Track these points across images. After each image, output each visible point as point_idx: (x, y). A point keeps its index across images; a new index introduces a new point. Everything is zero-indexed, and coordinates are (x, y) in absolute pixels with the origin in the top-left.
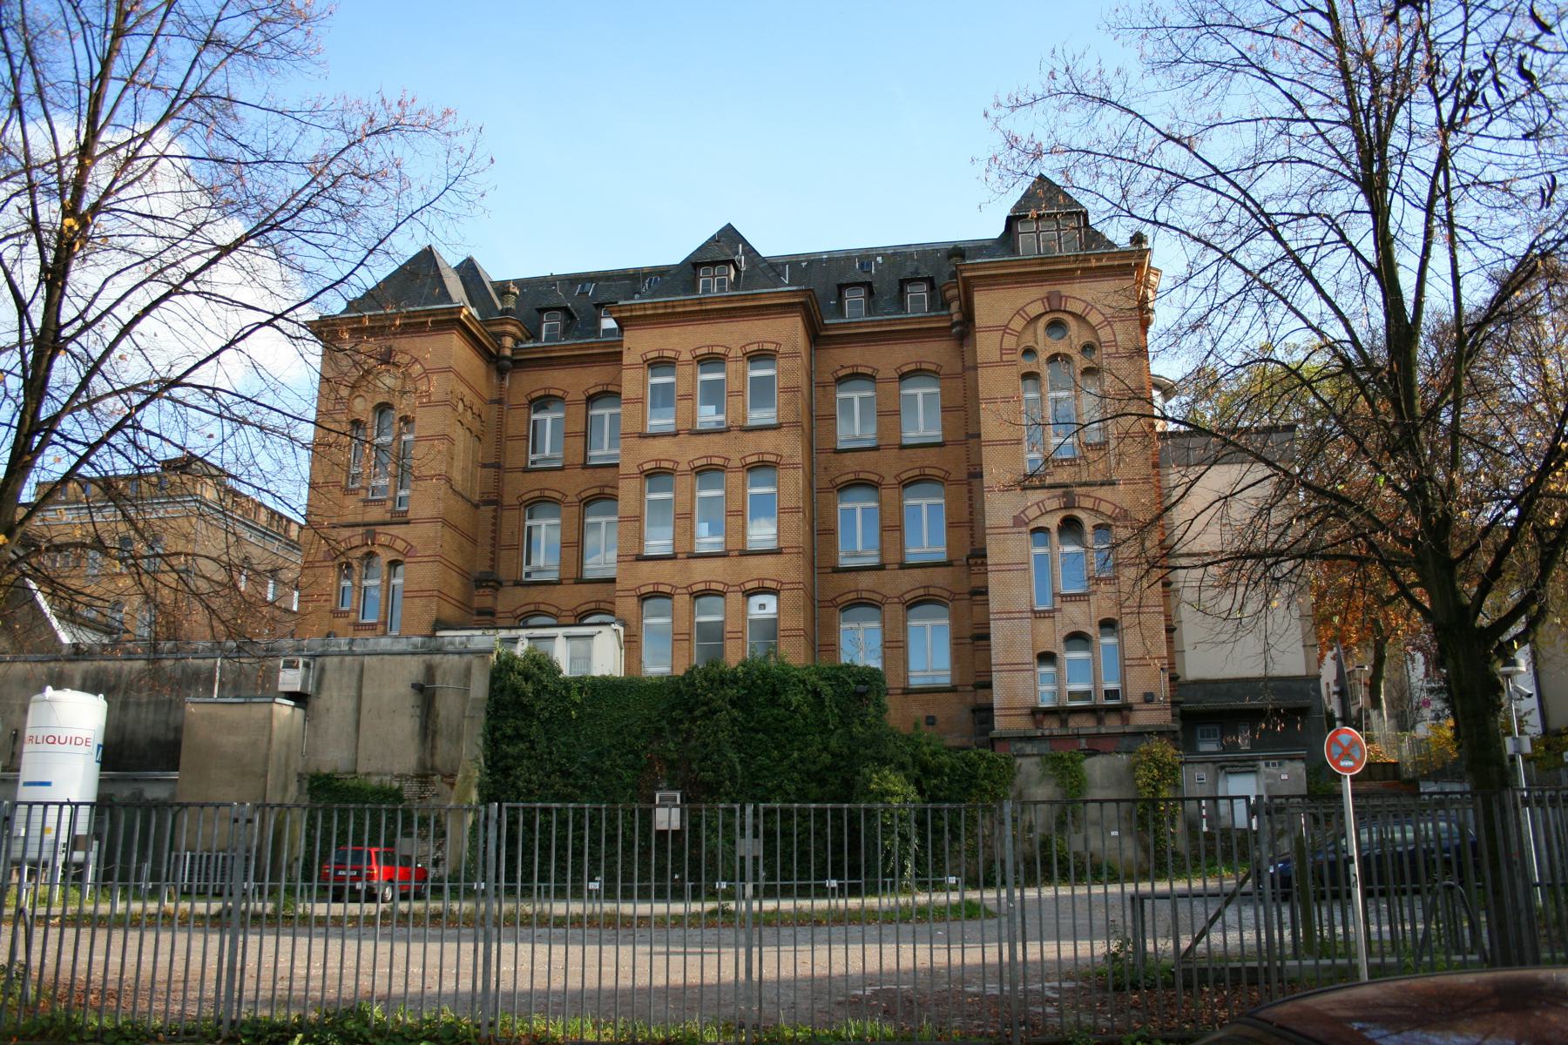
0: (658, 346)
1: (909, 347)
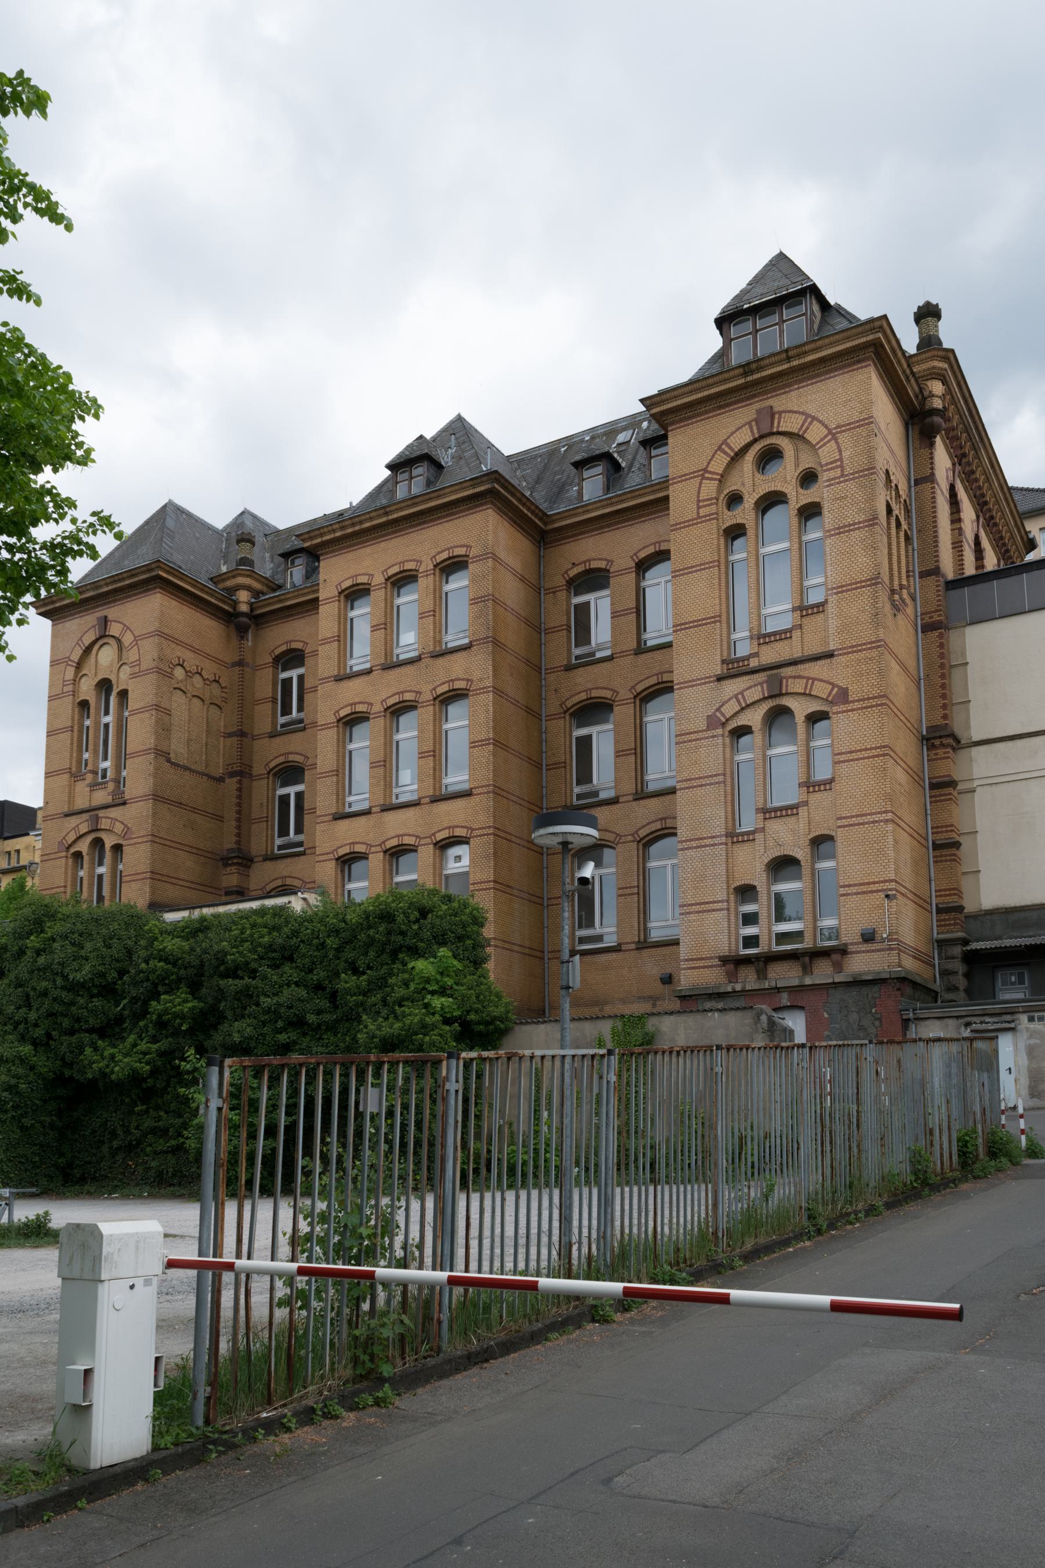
0: (352, 573)
1: (647, 526)
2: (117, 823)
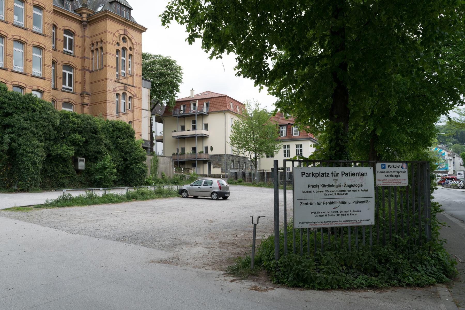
1: (67, 21)
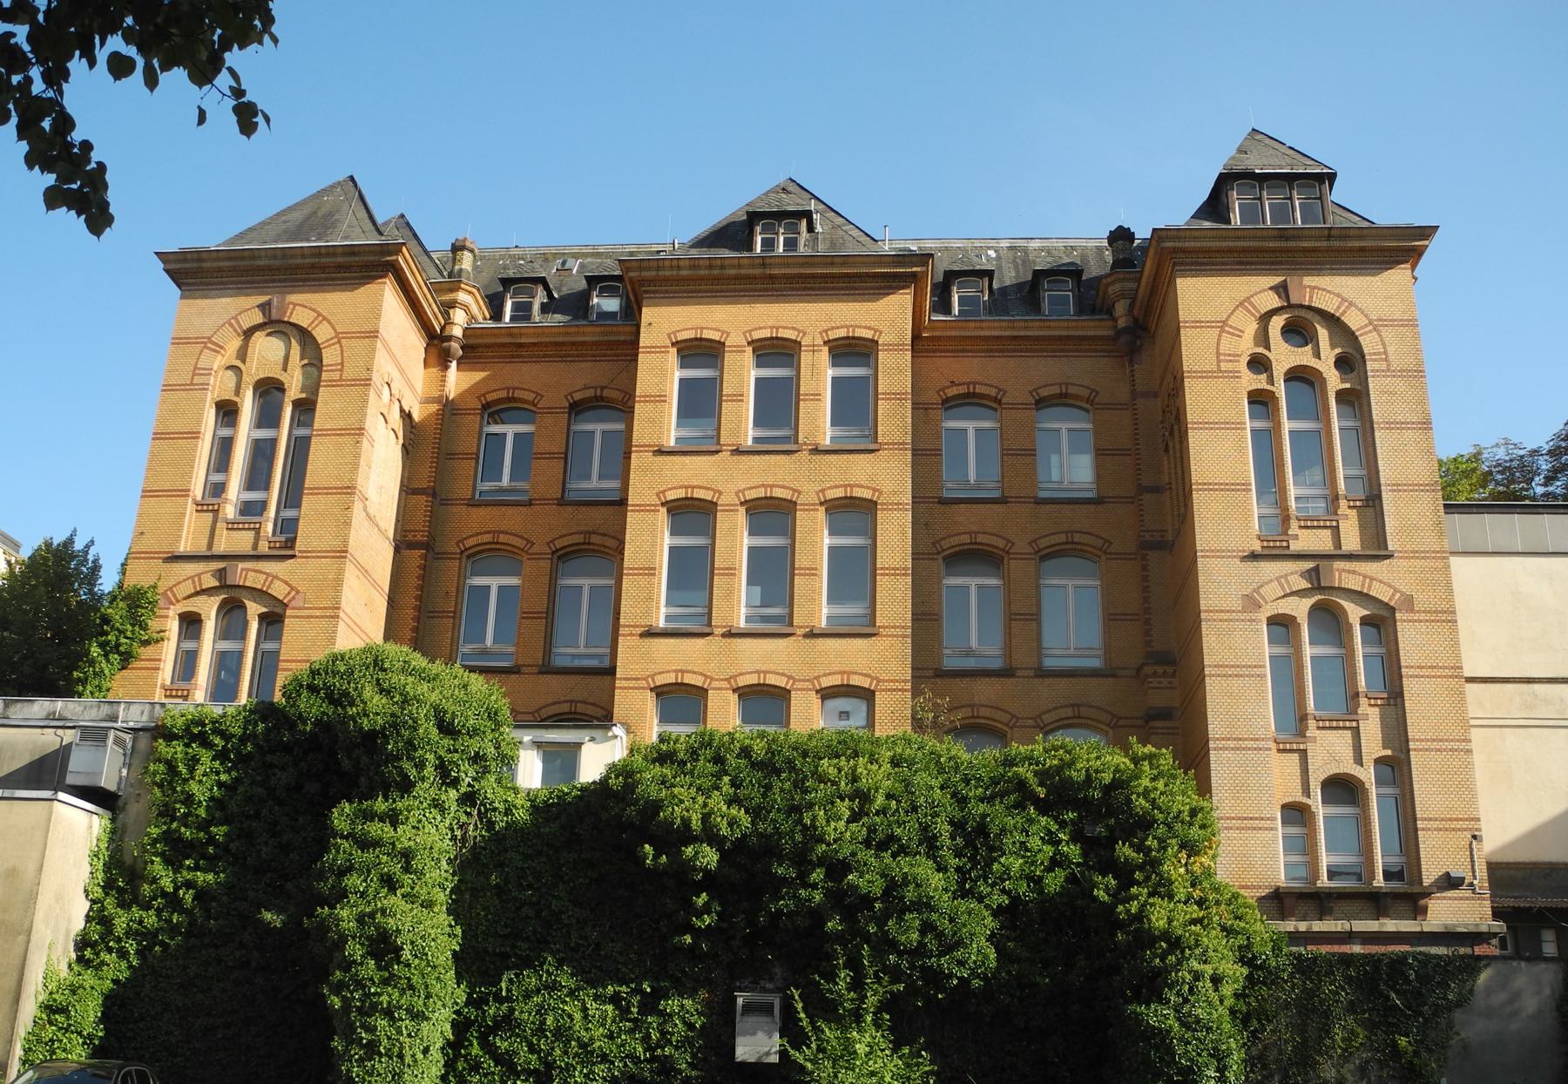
2: (277, 583)
